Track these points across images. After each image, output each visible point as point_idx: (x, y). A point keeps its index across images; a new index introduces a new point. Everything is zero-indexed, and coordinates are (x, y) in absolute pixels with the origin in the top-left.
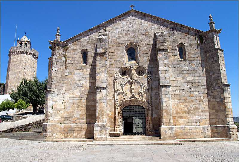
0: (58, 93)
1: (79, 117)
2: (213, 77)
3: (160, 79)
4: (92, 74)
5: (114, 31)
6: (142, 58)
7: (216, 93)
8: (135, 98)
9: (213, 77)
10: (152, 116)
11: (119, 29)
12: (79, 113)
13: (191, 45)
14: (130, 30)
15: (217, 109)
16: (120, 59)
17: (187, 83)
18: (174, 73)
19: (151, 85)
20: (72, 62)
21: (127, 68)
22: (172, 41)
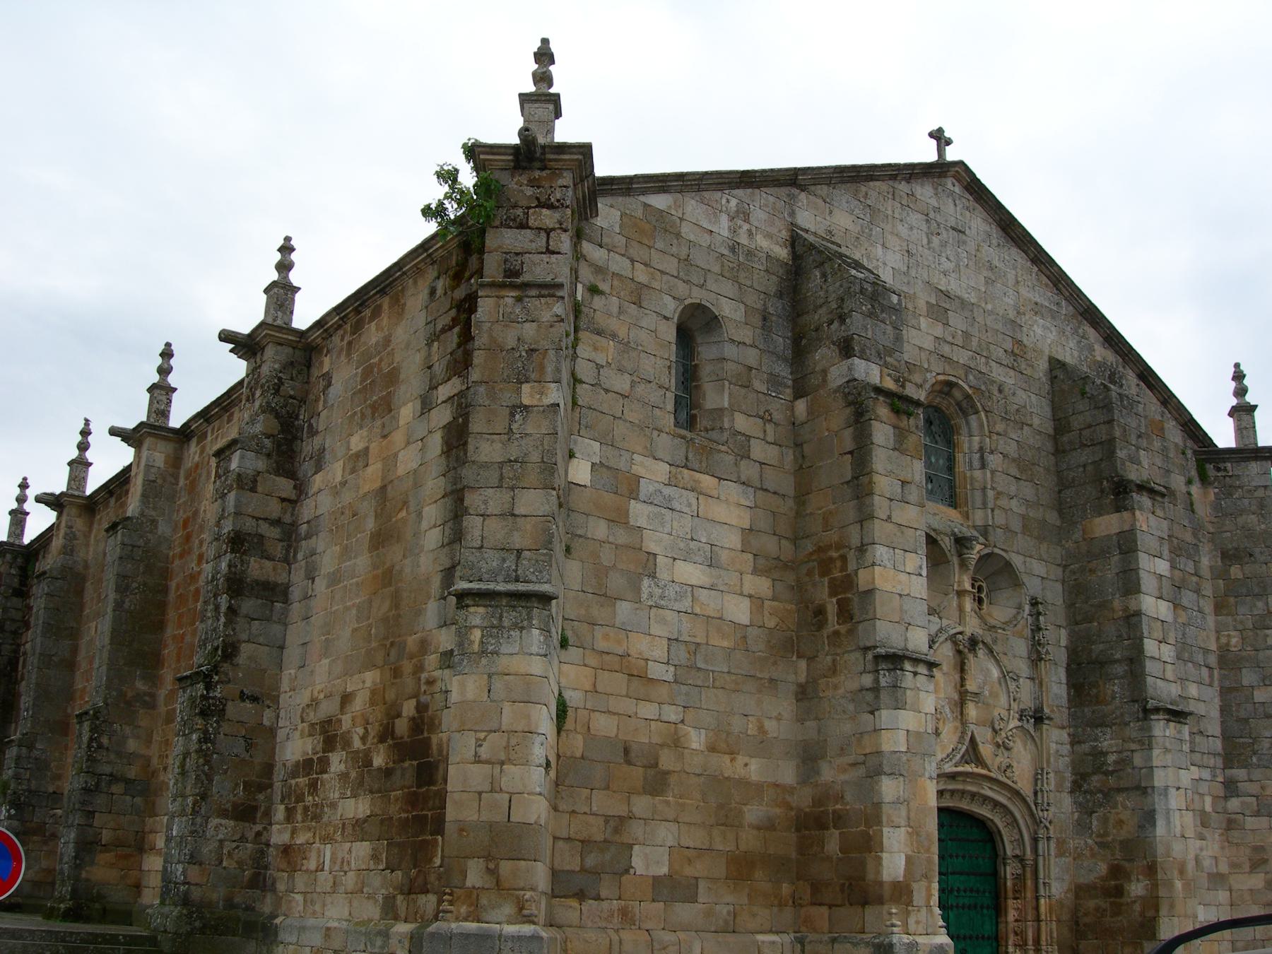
1: (664, 870)
3: (1150, 667)
4: (751, 530)
9: (1260, 696)
12: (666, 834)
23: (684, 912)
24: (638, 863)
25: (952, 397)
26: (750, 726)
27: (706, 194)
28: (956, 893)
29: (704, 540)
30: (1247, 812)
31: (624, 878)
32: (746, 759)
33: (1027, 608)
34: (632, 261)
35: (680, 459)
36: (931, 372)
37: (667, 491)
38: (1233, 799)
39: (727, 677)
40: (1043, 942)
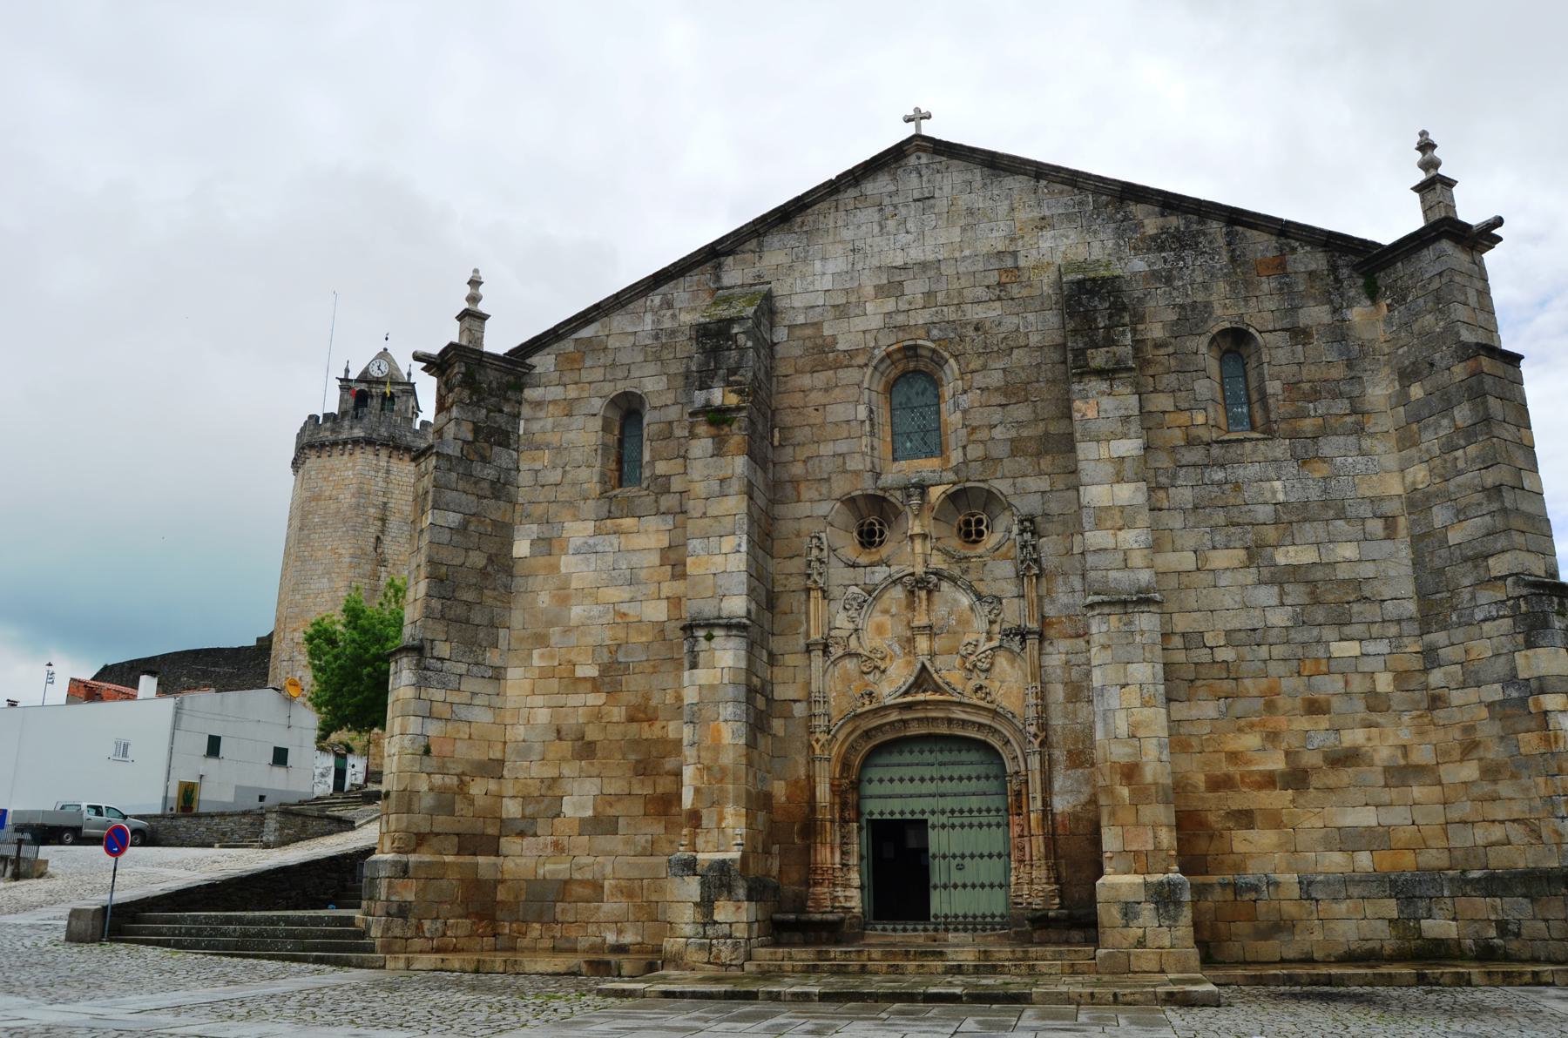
0: (462, 668)
1: (590, 813)
2: (1454, 537)
4: (670, 547)
5: (803, 277)
6: (978, 436)
7: (1481, 649)
8: (938, 689)
9: (1454, 537)
10: (1047, 803)
11: (838, 264)
12: (591, 787)
13: (1299, 334)
14: (899, 262)
15: (1490, 756)
16: (842, 447)
17: (1276, 589)
18: (1192, 520)
19: (1041, 607)
20: (555, 476)
21: (884, 499)
22: (1172, 316)
23: (603, 841)
24: (568, 809)
25: (922, 356)
26: (668, 697)
27: (631, 306)
28: (949, 815)
29: (624, 567)
30: (1453, 685)
31: (556, 820)
32: (664, 723)
33: (1015, 529)
34: (565, 385)
35: (604, 512)
36: (879, 347)
37: (591, 541)
38: (1435, 671)
39: (645, 664)
40: (1034, 858)
